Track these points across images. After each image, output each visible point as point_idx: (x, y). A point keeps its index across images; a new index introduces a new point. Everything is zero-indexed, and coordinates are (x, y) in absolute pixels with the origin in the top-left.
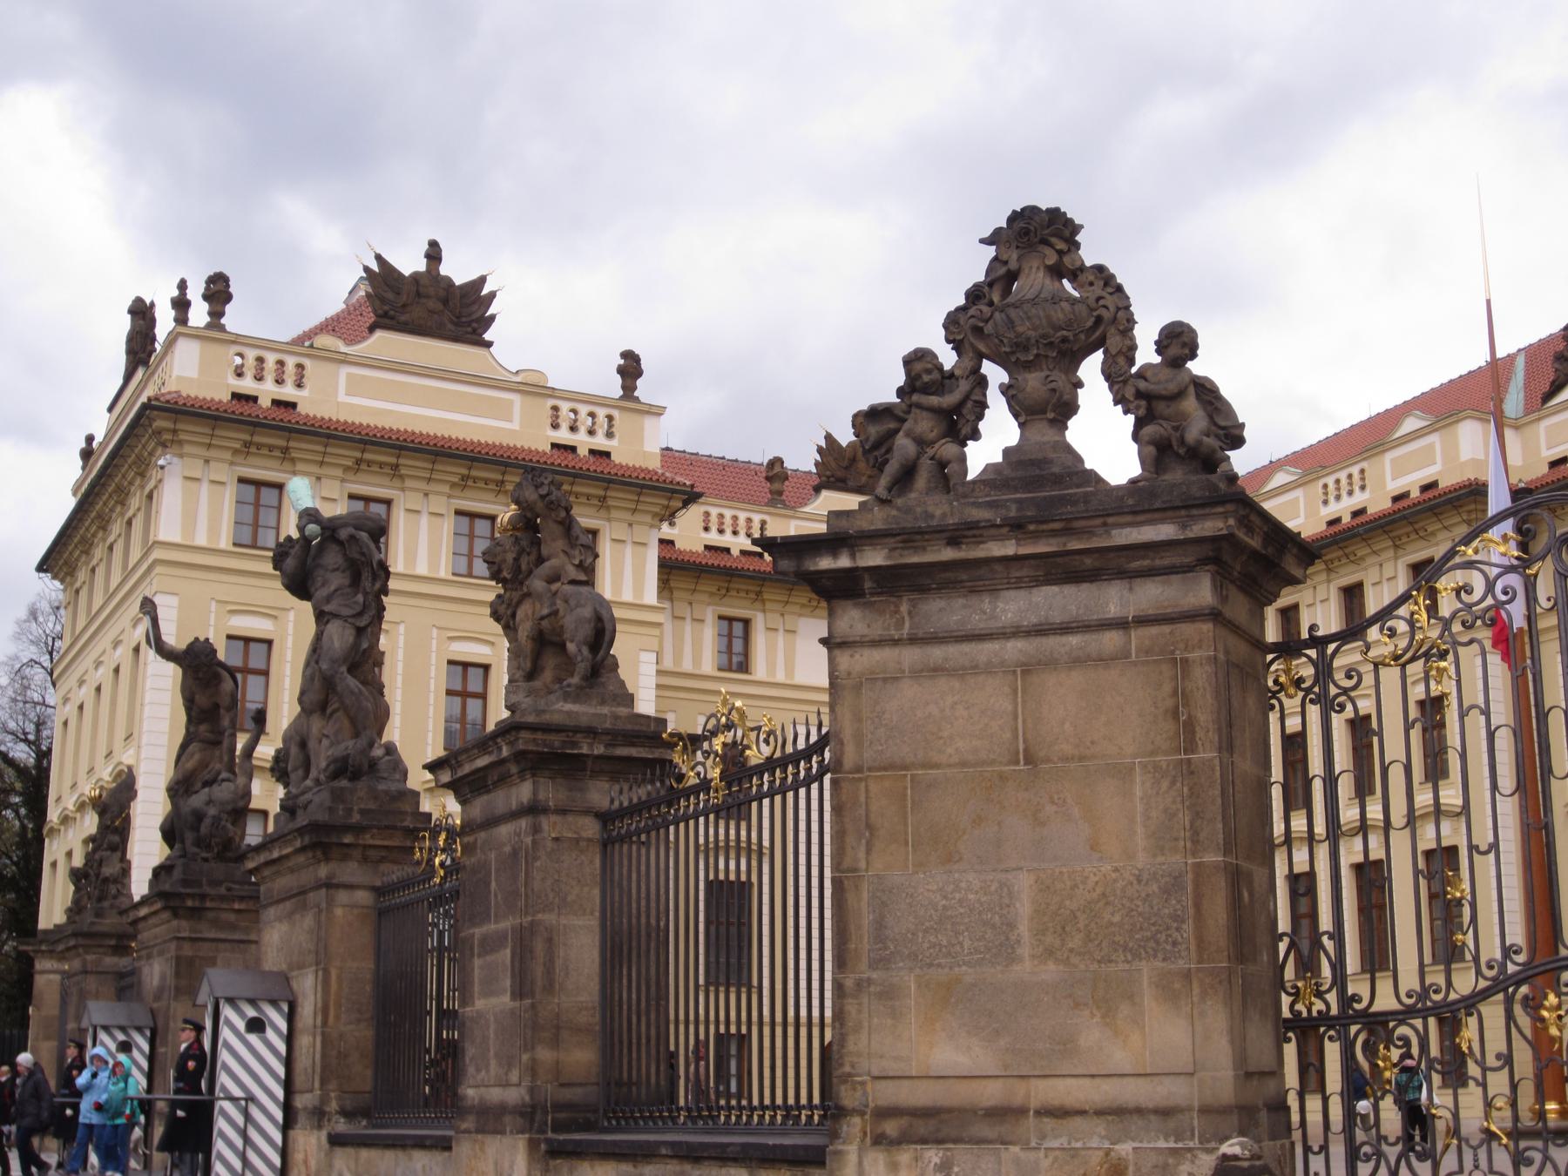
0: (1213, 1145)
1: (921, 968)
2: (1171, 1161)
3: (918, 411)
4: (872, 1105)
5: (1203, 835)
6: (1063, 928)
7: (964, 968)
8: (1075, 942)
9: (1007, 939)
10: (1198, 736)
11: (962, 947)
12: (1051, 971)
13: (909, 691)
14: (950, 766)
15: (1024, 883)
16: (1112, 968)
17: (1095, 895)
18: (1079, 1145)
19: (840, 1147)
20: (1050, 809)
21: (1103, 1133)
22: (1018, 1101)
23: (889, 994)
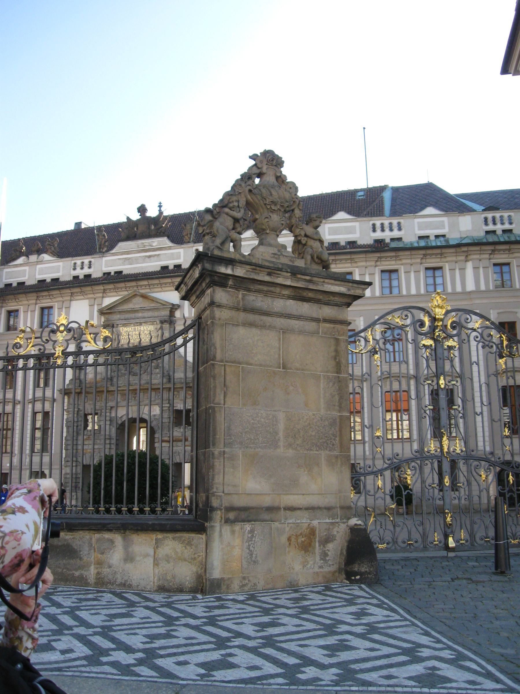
0: (345, 521)
1: (244, 448)
2: (331, 527)
3: (226, 216)
4: (223, 506)
5: (343, 405)
6: (295, 436)
7: (259, 449)
8: (299, 442)
9: (275, 438)
10: (342, 368)
11: (259, 440)
12: (290, 452)
13: (242, 331)
14: (256, 365)
15: (281, 416)
16: (312, 452)
17: (306, 424)
18: (299, 521)
19: (212, 524)
20: (291, 388)
21: (308, 517)
22: (276, 504)
23: (232, 458)
